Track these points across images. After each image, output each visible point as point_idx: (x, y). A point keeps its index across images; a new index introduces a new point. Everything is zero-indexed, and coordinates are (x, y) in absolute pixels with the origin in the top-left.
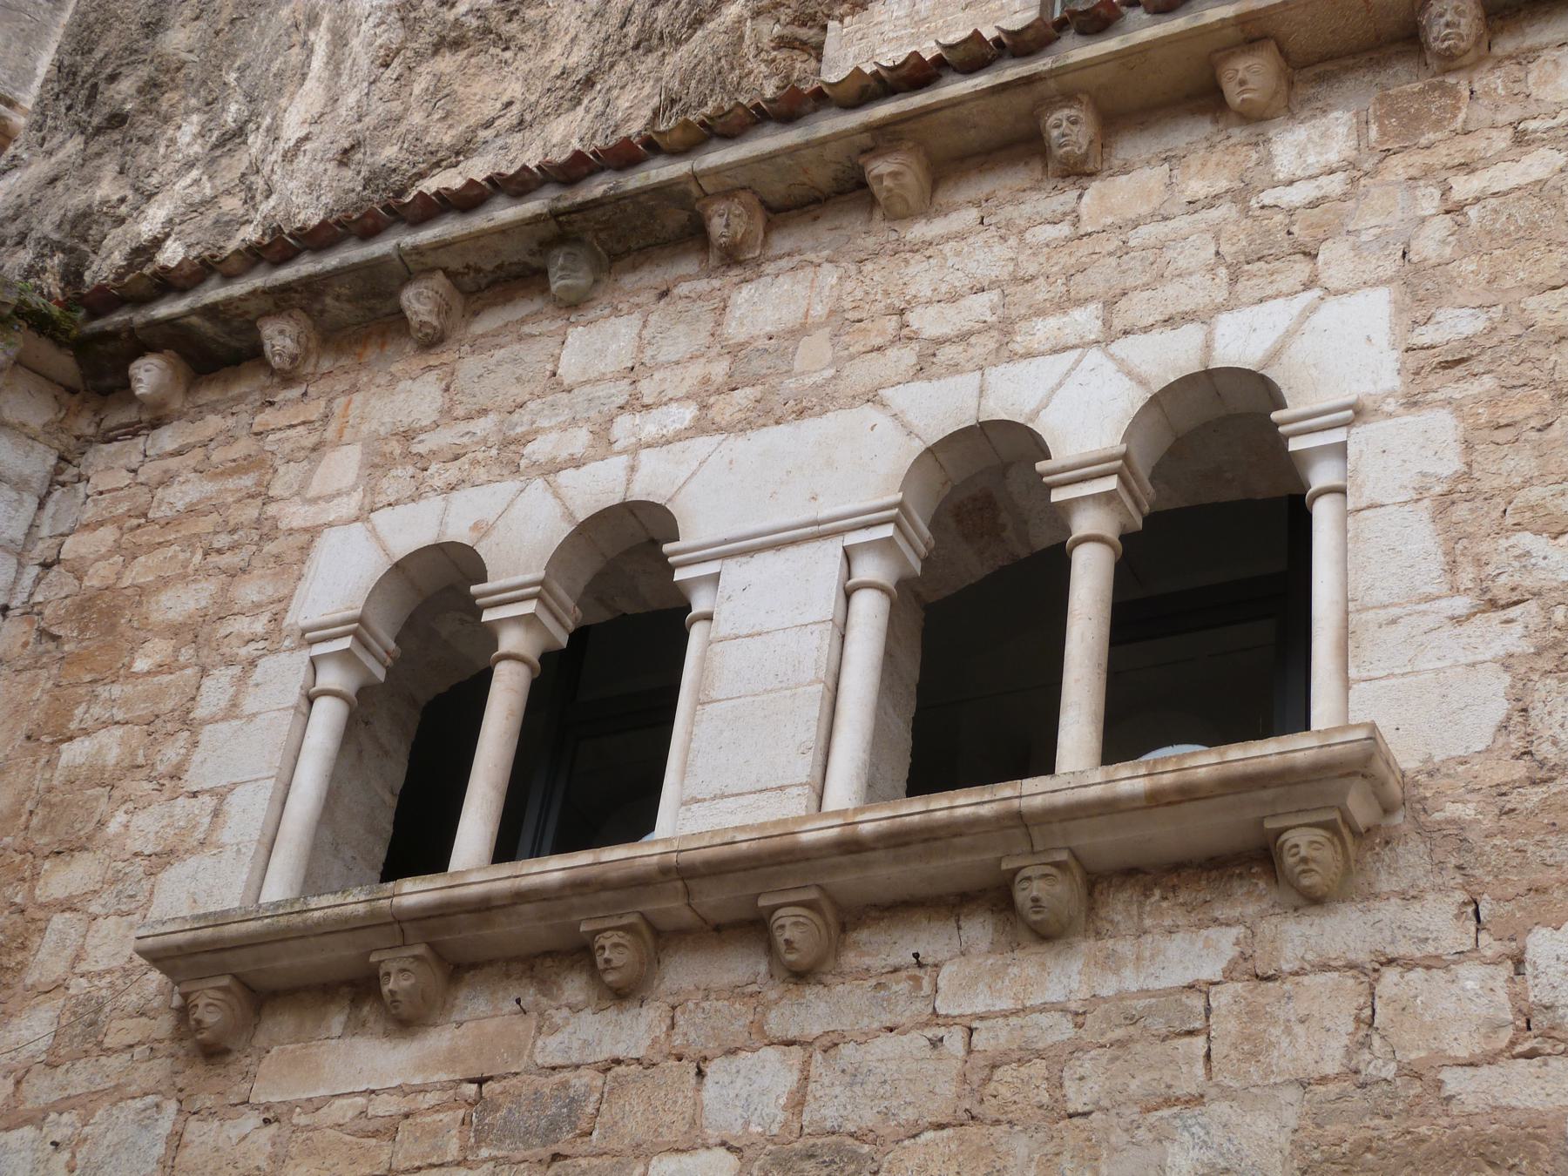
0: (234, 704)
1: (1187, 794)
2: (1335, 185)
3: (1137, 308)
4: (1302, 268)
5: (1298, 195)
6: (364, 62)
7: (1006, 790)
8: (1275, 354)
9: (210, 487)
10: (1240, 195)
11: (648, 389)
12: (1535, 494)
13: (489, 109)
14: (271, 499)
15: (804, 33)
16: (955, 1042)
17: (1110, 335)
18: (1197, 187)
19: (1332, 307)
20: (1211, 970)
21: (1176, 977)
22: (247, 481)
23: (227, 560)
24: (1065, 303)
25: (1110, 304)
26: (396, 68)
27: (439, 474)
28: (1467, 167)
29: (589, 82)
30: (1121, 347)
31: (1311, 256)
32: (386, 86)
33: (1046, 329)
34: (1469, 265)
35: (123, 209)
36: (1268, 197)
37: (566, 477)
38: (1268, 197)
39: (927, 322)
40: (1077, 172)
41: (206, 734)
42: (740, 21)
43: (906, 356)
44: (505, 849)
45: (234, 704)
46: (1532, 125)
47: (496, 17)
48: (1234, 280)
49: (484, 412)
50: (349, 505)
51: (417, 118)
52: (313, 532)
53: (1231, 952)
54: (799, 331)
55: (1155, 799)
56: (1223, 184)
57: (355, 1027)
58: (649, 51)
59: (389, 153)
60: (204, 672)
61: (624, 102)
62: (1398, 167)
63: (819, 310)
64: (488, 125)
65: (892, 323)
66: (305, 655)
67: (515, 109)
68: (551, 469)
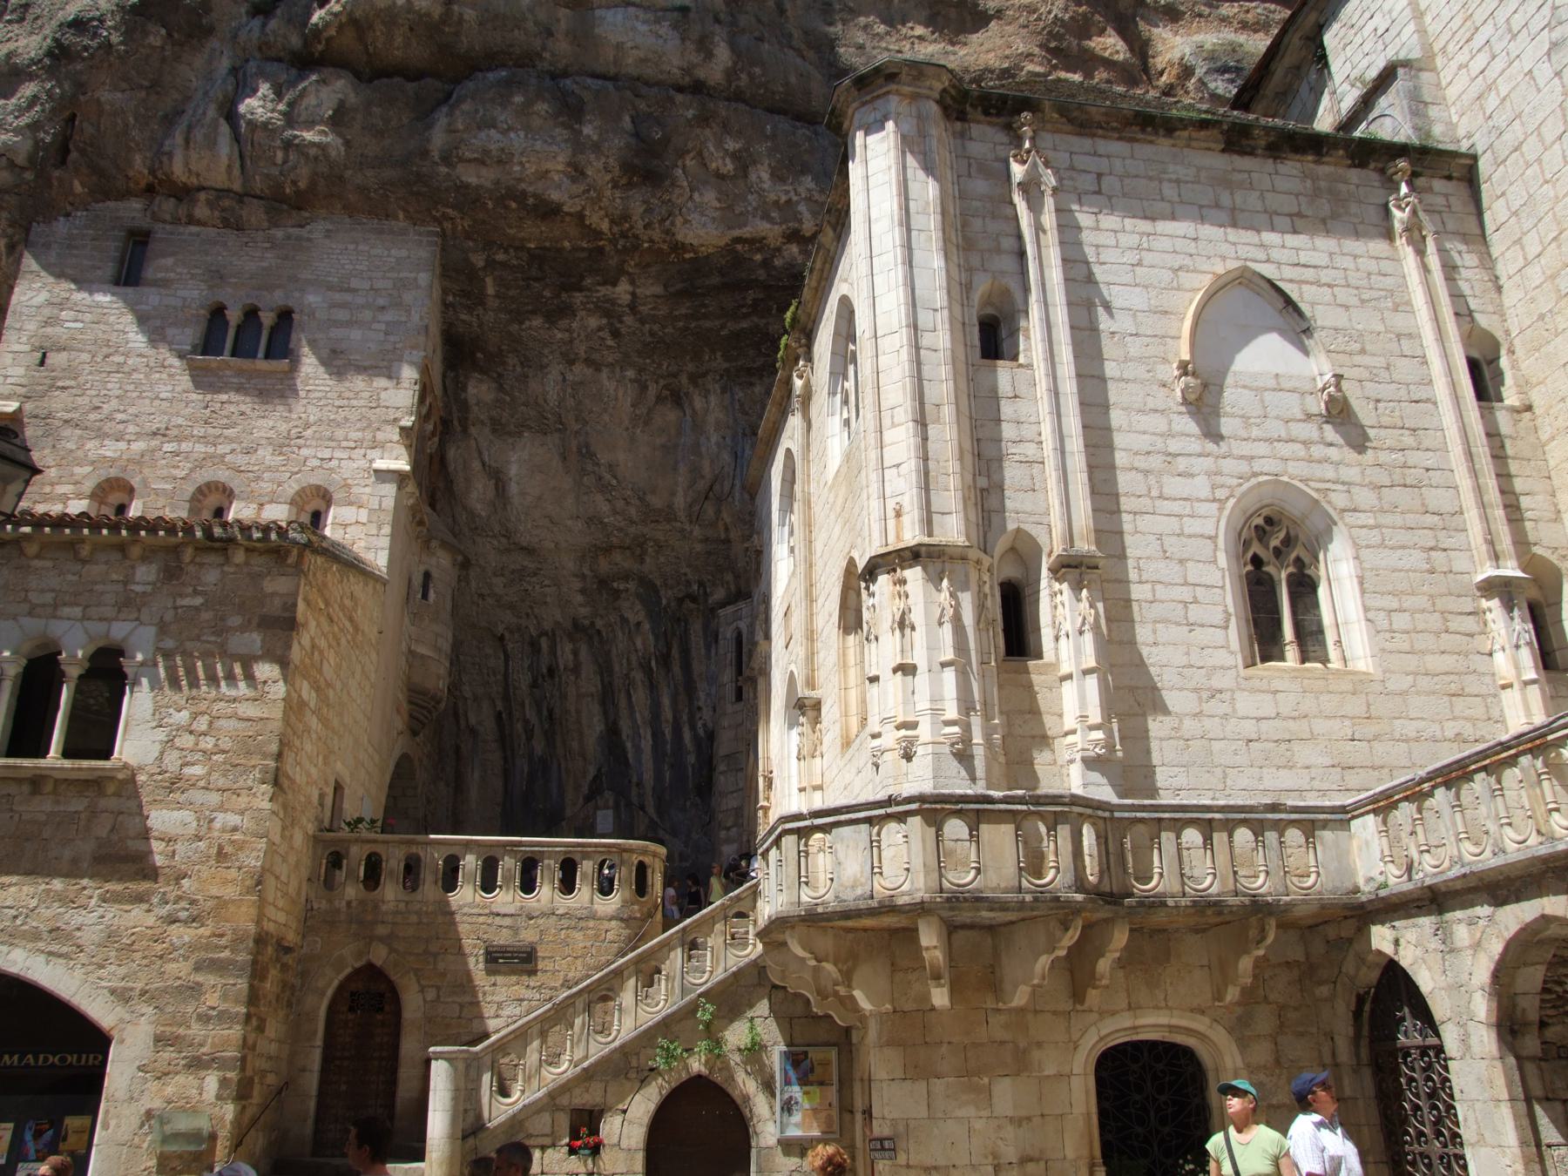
2: (149, 588)
5: (138, 588)
7: (36, 761)
10: (125, 583)
16: (16, 817)
17: (85, 618)
18: (115, 577)
19: (141, 629)
20: (81, 808)
21: (72, 809)
25: (86, 607)
28: (181, 596)
33: (66, 611)
39: (34, 597)
43: (25, 607)
65: (23, 594)
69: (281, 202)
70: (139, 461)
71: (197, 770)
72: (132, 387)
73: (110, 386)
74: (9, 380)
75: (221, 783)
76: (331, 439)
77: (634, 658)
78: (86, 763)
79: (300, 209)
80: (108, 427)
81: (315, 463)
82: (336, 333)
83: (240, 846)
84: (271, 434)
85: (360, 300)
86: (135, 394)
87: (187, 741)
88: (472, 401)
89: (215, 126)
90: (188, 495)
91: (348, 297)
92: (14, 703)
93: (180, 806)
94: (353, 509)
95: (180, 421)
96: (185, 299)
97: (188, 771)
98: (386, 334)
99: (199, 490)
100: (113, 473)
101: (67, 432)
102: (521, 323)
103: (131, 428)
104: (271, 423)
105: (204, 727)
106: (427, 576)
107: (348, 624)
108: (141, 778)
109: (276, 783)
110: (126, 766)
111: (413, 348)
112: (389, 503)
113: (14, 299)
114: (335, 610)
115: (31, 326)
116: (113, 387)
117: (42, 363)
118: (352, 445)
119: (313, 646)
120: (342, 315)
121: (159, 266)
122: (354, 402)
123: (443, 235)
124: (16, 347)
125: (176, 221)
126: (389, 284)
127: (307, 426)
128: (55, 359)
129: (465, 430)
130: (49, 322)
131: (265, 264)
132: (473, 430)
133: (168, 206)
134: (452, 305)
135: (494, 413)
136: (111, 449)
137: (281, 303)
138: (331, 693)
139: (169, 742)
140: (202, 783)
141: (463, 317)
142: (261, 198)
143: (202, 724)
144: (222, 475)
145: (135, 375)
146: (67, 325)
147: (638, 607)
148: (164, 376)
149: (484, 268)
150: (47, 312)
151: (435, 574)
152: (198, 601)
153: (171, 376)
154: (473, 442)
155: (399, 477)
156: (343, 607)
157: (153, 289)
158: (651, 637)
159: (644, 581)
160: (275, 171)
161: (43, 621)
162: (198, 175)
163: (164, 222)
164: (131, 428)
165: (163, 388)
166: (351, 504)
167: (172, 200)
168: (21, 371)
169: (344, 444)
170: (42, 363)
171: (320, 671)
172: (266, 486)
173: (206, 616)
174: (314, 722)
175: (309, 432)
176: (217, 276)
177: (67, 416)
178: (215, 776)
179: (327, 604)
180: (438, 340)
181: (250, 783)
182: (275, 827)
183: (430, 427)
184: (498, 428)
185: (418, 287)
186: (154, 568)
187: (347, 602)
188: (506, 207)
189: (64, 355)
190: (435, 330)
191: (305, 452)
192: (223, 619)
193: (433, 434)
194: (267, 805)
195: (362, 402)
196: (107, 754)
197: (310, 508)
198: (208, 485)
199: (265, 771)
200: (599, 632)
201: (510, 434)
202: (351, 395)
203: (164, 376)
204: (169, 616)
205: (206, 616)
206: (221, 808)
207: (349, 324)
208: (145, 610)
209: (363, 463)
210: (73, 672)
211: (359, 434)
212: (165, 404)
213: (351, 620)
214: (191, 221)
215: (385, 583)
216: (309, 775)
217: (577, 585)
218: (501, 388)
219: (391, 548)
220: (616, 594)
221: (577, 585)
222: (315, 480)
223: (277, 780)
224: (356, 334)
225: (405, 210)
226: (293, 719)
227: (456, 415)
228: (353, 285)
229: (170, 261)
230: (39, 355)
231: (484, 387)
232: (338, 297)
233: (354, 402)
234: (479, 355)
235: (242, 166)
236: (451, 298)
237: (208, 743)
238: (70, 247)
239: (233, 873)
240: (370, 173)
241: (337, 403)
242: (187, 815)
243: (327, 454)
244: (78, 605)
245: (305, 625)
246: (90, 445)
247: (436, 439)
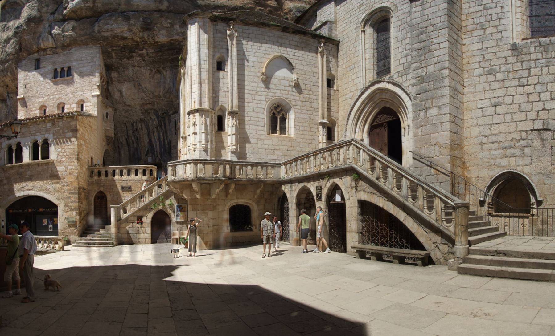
5: (48, 128)
10: (46, 127)
33: (37, 134)
70: (46, 101)
71: (64, 159)
77: (154, 126)
78: (45, 160)
80: (40, 96)
81: (80, 95)
83: (73, 172)
87: (61, 154)
88: (113, 77)
90: (56, 106)
93: (62, 166)
97: (62, 159)
99: (58, 104)
100: (42, 104)
101: (32, 98)
103: (44, 95)
108: (55, 161)
109: (78, 160)
110: (52, 160)
112: (96, 101)
114: (86, 125)
119: (82, 133)
121: (43, 64)
127: (77, 88)
129: (112, 83)
132: (114, 83)
136: (41, 100)
138: (87, 141)
143: (63, 151)
144: (62, 101)
147: (154, 115)
152: (59, 128)
155: (98, 96)
156: (87, 124)
158: (157, 121)
159: (154, 110)
164: (44, 95)
171: (84, 137)
172: (71, 101)
173: (61, 131)
174: (84, 147)
179: (84, 124)
180: (104, 66)
182: (79, 168)
183: (104, 84)
184: (119, 82)
186: (50, 124)
187: (88, 123)
191: (78, 93)
193: (105, 85)
194: (77, 164)
196: (48, 158)
197: (81, 104)
198: (60, 103)
199: (76, 158)
200: (146, 121)
201: (122, 82)
204: (54, 132)
205: (61, 131)
206: (69, 165)
209: (90, 94)
210: (40, 144)
213: (90, 126)
215: (97, 117)
216: (85, 157)
217: (140, 112)
218: (119, 74)
220: (149, 113)
221: (140, 112)
222: (81, 98)
223: (78, 159)
226: (80, 148)
227: (110, 80)
231: (115, 74)
237: (65, 154)
239: (73, 177)
242: (63, 167)
243: (82, 93)
245: (80, 130)
246: (37, 100)
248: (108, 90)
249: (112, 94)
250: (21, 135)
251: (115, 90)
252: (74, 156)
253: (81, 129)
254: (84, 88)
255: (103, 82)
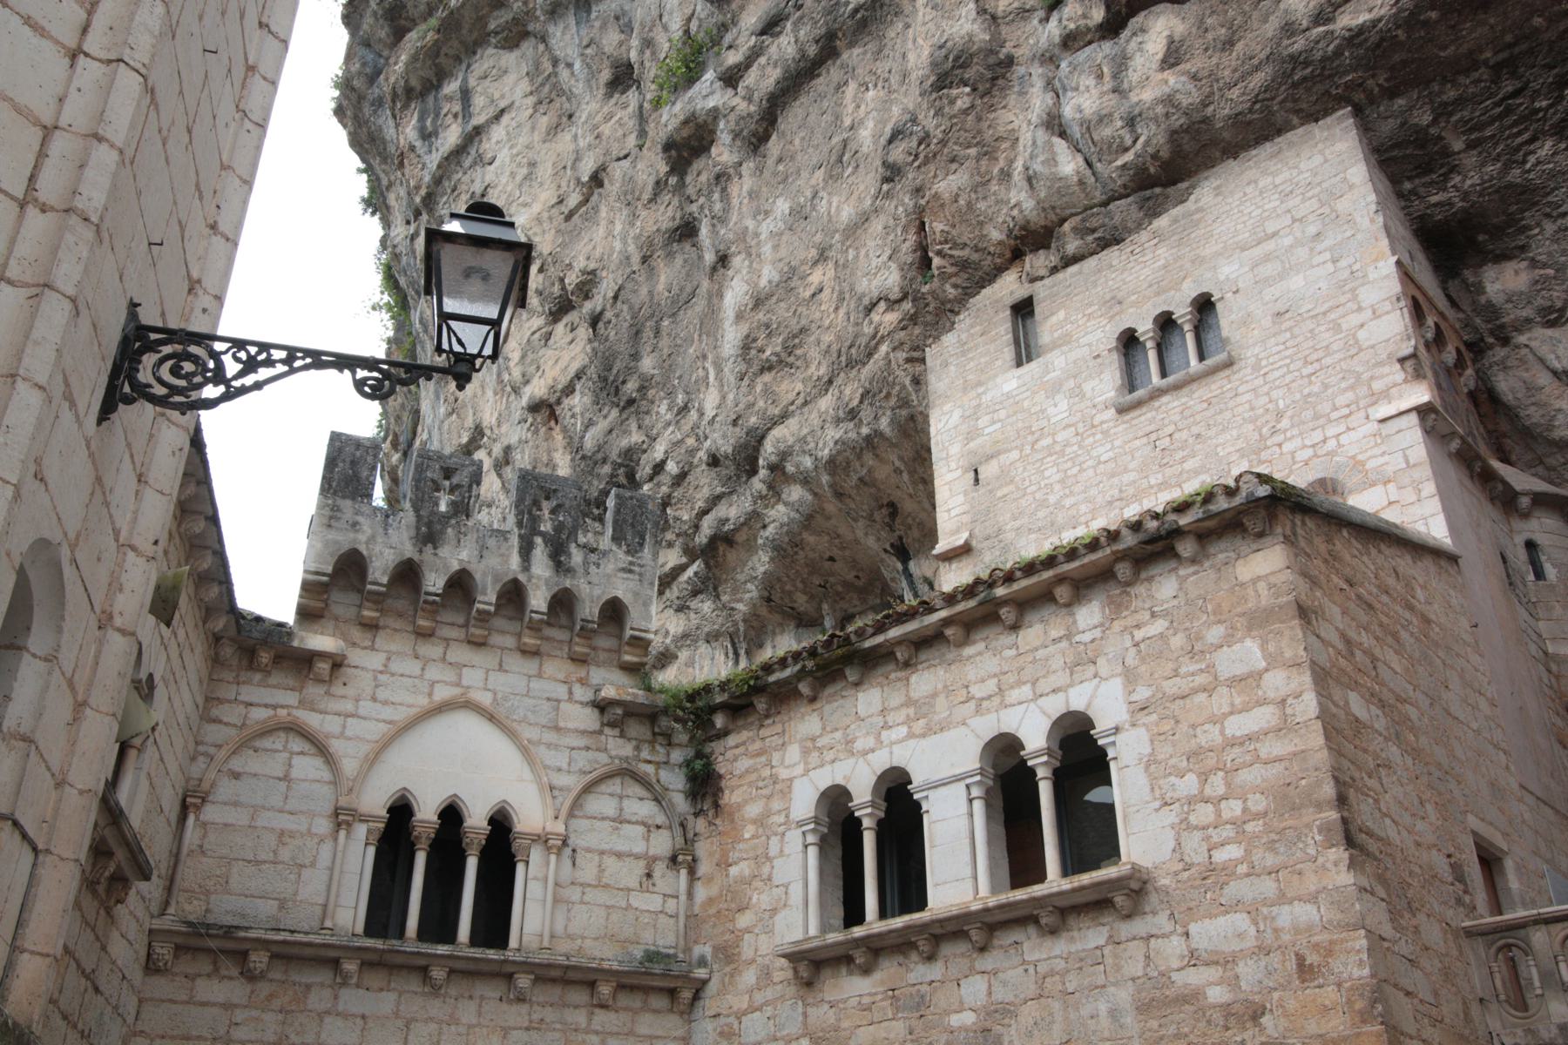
0: (782, 851)
1: (1082, 888)
2: (1097, 633)
3: (1043, 686)
4: (1091, 669)
5: (1087, 637)
6: (732, 379)
8: (1089, 705)
9: (751, 762)
10: (1068, 636)
11: (890, 719)
12: (1173, 761)
13: (791, 396)
14: (772, 767)
15: (916, 354)
16: (1031, 970)
18: (1054, 634)
19: (1104, 686)
20: (1102, 942)
21: (1092, 945)
22: (763, 759)
23: (764, 792)
24: (1020, 683)
25: (1034, 684)
26: (746, 381)
27: (829, 756)
28: (1138, 627)
29: (830, 382)
30: (1041, 701)
31: (1095, 663)
32: (744, 389)
33: (1014, 695)
34: (1143, 668)
35: (645, 446)
36: (1077, 638)
37: (870, 756)
38: (1077, 638)
39: (977, 691)
40: (1015, 627)
41: (775, 862)
42: (888, 353)
43: (972, 705)
44: (883, 914)
45: (782, 851)
46: (1156, 609)
47: (783, 355)
48: (1071, 674)
49: (837, 729)
50: (799, 769)
51: (761, 403)
52: (791, 780)
53: (1106, 935)
54: (934, 695)
55: (1074, 890)
56: (1062, 633)
57: (850, 973)
58: (852, 368)
59: (753, 420)
60: (768, 838)
61: (848, 392)
62: (1117, 626)
63: (940, 686)
64: (792, 403)
66: (799, 831)
67: (802, 395)
68: (865, 753)
69: (1152, 187)
71: (1232, 852)
72: (1070, 464)
73: (1047, 474)
74: (953, 513)
75: (1270, 860)
76: (1316, 417)
79: (1174, 183)
81: (1307, 453)
82: (1269, 293)
83: (1329, 951)
84: (1241, 444)
85: (1288, 241)
86: (1075, 470)
87: (1204, 813)
89: (1050, 146)
91: (1270, 246)
92: (1001, 831)
93: (1226, 909)
94: (1379, 489)
95: (1132, 476)
96: (1090, 345)
98: (1334, 261)
102: (1524, 162)
104: (1235, 433)
105: (1221, 790)
106: (1531, 546)
107: (1407, 615)
109: (1350, 842)
110: (1136, 869)
111: (1376, 260)
113: (933, 431)
115: (955, 449)
116: (1052, 474)
117: (977, 480)
118: (1346, 411)
120: (1269, 269)
122: (1328, 361)
123: (1358, 112)
124: (949, 477)
125: (1054, 270)
126: (1314, 204)
127: (1280, 415)
128: (986, 472)
129: (1505, 341)
130: (971, 436)
131: (1162, 262)
133: (1038, 261)
134: (1413, 192)
135: (1539, 302)
137: (1194, 294)
139: (1184, 825)
140: (1242, 869)
141: (1434, 199)
142: (1127, 196)
143: (1217, 785)
145: (1068, 450)
146: (987, 431)
148: (1099, 436)
149: (1435, 121)
150: (964, 428)
151: (1540, 538)
153: (1105, 433)
154: (1524, 351)
157: (1056, 352)
160: (1129, 157)
161: (994, 716)
162: (1053, 208)
163: (1042, 278)
164: (1083, 508)
165: (1101, 450)
166: (1373, 485)
167: (1041, 252)
168: (961, 498)
169: (1335, 415)
170: (977, 480)
175: (1285, 423)
176: (1116, 302)
177: (1017, 524)
178: (1257, 856)
181: (1312, 851)
182: (1380, 919)
185: (1351, 187)
187: (1391, 581)
188: (1426, 23)
189: (994, 462)
190: (1403, 232)
191: (1287, 447)
192: (1199, 638)
194: (1345, 878)
195: (1338, 356)
199: (1325, 829)
202: (1321, 354)
203: (1099, 436)
204: (1131, 659)
205: (1177, 641)
206: (1282, 899)
207: (1281, 277)
208: (1101, 661)
211: (1350, 395)
212: (1112, 465)
213: (1411, 608)
214: (1069, 261)
218: (1534, 264)
219: (1445, 509)
223: (1350, 837)
224: (1296, 282)
225: (1297, 112)
228: (1270, 230)
229: (1061, 314)
230: (972, 474)
232: (1257, 252)
233: (1328, 361)
234: (1481, 238)
235: (1094, 174)
236: (1408, 186)
237: (1233, 808)
238: (964, 353)
239: (1330, 995)
240: (1234, 93)
241: (1306, 371)
242: (1241, 921)
243: (1317, 436)
244: (1024, 683)
247: (1469, 372)
248: (1493, 398)
249: (1533, 416)
250: (908, 721)
251: (1544, 379)
252: (1309, 815)
253: (1335, 611)
254: (1325, 407)
255: (1439, 340)
